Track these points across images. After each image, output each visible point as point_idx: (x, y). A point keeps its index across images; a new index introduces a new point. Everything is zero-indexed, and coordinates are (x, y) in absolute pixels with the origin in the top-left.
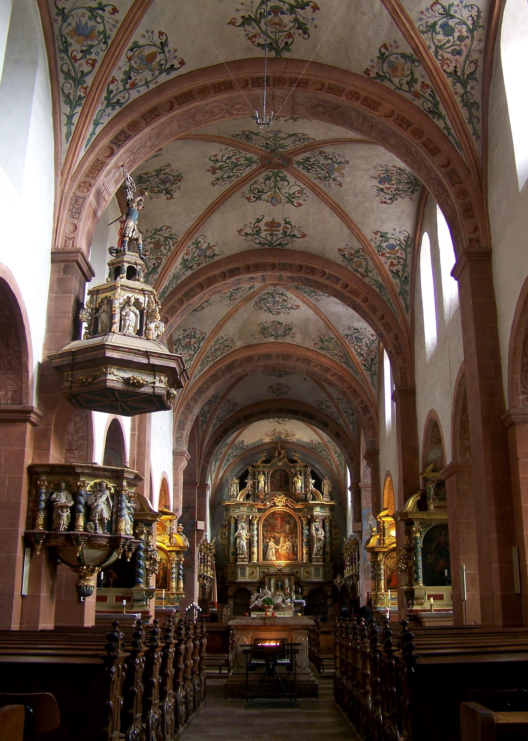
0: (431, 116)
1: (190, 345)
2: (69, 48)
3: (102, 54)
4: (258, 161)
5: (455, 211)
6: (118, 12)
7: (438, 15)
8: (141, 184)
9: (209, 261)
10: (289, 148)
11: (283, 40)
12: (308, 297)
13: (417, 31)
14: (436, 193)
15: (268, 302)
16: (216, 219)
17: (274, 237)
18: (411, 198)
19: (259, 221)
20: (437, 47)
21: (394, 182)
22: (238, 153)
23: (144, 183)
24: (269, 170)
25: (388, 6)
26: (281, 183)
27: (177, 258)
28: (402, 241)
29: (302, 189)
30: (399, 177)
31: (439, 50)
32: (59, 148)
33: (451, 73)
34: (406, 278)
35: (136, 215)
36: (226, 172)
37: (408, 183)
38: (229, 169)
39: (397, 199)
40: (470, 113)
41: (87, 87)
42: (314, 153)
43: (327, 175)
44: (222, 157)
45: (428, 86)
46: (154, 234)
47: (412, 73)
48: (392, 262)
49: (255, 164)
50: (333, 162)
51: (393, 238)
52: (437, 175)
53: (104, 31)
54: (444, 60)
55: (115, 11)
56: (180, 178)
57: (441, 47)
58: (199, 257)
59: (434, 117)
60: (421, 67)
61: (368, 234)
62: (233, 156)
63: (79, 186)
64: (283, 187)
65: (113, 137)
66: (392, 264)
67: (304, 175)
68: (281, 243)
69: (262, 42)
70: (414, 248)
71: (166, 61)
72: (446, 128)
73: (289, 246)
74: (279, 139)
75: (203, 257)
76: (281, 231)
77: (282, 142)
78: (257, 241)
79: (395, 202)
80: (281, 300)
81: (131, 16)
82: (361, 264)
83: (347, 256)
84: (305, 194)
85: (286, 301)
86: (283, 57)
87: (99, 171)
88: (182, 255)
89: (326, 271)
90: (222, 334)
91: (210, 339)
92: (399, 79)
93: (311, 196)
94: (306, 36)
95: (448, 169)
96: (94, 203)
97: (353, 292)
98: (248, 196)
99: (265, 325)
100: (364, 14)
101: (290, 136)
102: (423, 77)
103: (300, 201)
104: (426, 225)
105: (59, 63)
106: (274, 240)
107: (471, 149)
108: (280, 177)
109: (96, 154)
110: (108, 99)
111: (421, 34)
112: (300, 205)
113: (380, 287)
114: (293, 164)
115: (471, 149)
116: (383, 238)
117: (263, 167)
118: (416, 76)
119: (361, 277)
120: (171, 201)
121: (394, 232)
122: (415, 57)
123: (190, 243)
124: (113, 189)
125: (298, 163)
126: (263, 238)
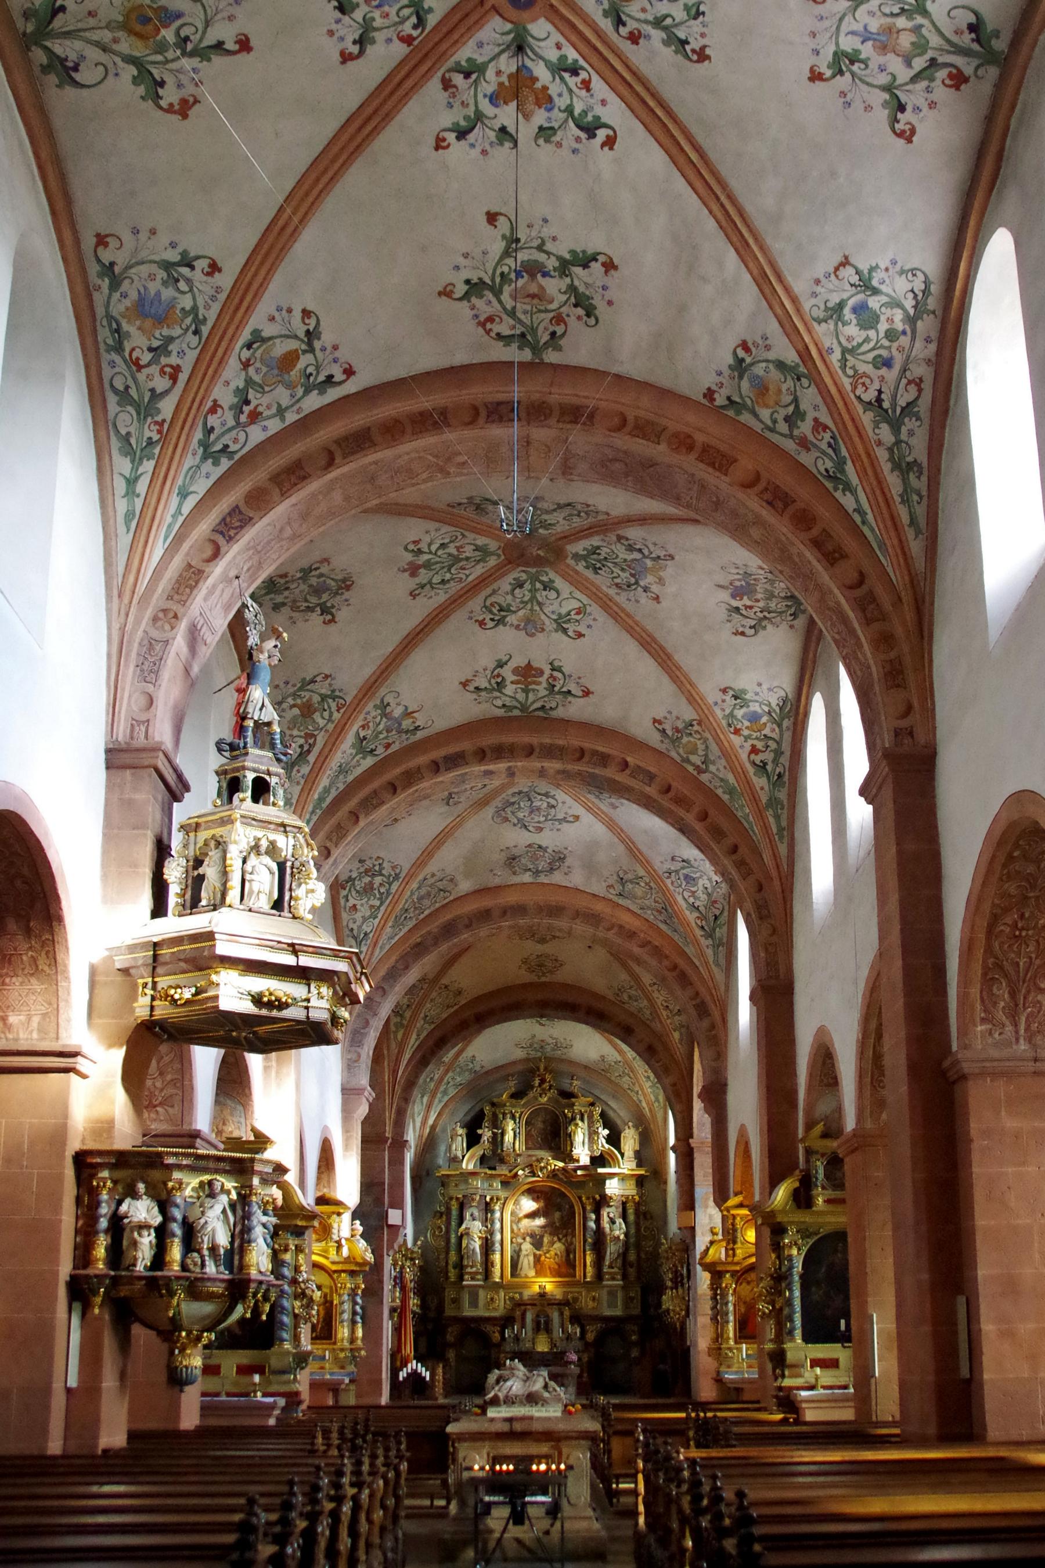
0: (829, 485)
1: (372, 889)
2: (126, 343)
3: (192, 355)
4: (500, 552)
5: (871, 674)
6: (220, 270)
7: (849, 287)
10: (559, 529)
11: (546, 329)
12: (596, 801)
13: (807, 317)
14: (837, 637)
15: (520, 808)
16: (419, 660)
18: (791, 627)
19: (501, 665)
20: (844, 351)
21: (759, 596)
23: (278, 592)
25: (751, 265)
26: (544, 593)
27: (347, 733)
30: (769, 588)
31: (848, 357)
32: (113, 543)
33: (870, 403)
34: (780, 775)
35: (265, 675)
37: (786, 598)
39: (764, 628)
40: (905, 481)
41: (164, 421)
43: (633, 580)
44: (429, 545)
45: (825, 428)
46: (301, 689)
47: (796, 401)
48: (753, 746)
49: (493, 558)
50: (644, 556)
52: (838, 603)
53: (195, 309)
54: (857, 377)
55: (214, 268)
57: (852, 351)
59: (836, 489)
60: (813, 390)
61: (709, 692)
63: (155, 619)
65: (217, 521)
66: (754, 750)
67: (587, 579)
69: (507, 332)
70: (796, 719)
71: (318, 368)
72: (859, 510)
73: (560, 713)
76: (545, 685)
77: (545, 517)
78: (499, 703)
79: (762, 633)
80: (545, 805)
81: (247, 279)
83: (669, 733)
85: (553, 807)
86: (547, 360)
87: (192, 588)
88: (355, 728)
89: (629, 759)
90: (433, 867)
91: (411, 876)
92: (770, 411)
93: (601, 619)
94: (592, 321)
95: (859, 592)
96: (184, 650)
97: (680, 801)
98: (481, 618)
99: (516, 852)
100: (704, 279)
101: (560, 507)
102: (816, 408)
104: (820, 680)
105: (107, 373)
106: (530, 700)
107: (904, 553)
109: (187, 554)
110: (205, 444)
111: (815, 324)
112: (580, 635)
113: (731, 791)
115: (904, 553)
117: (510, 563)
118: (803, 407)
119: (695, 773)
120: (332, 627)
121: (758, 689)
122: (802, 369)
123: (370, 706)
124: (221, 622)
125: (576, 557)
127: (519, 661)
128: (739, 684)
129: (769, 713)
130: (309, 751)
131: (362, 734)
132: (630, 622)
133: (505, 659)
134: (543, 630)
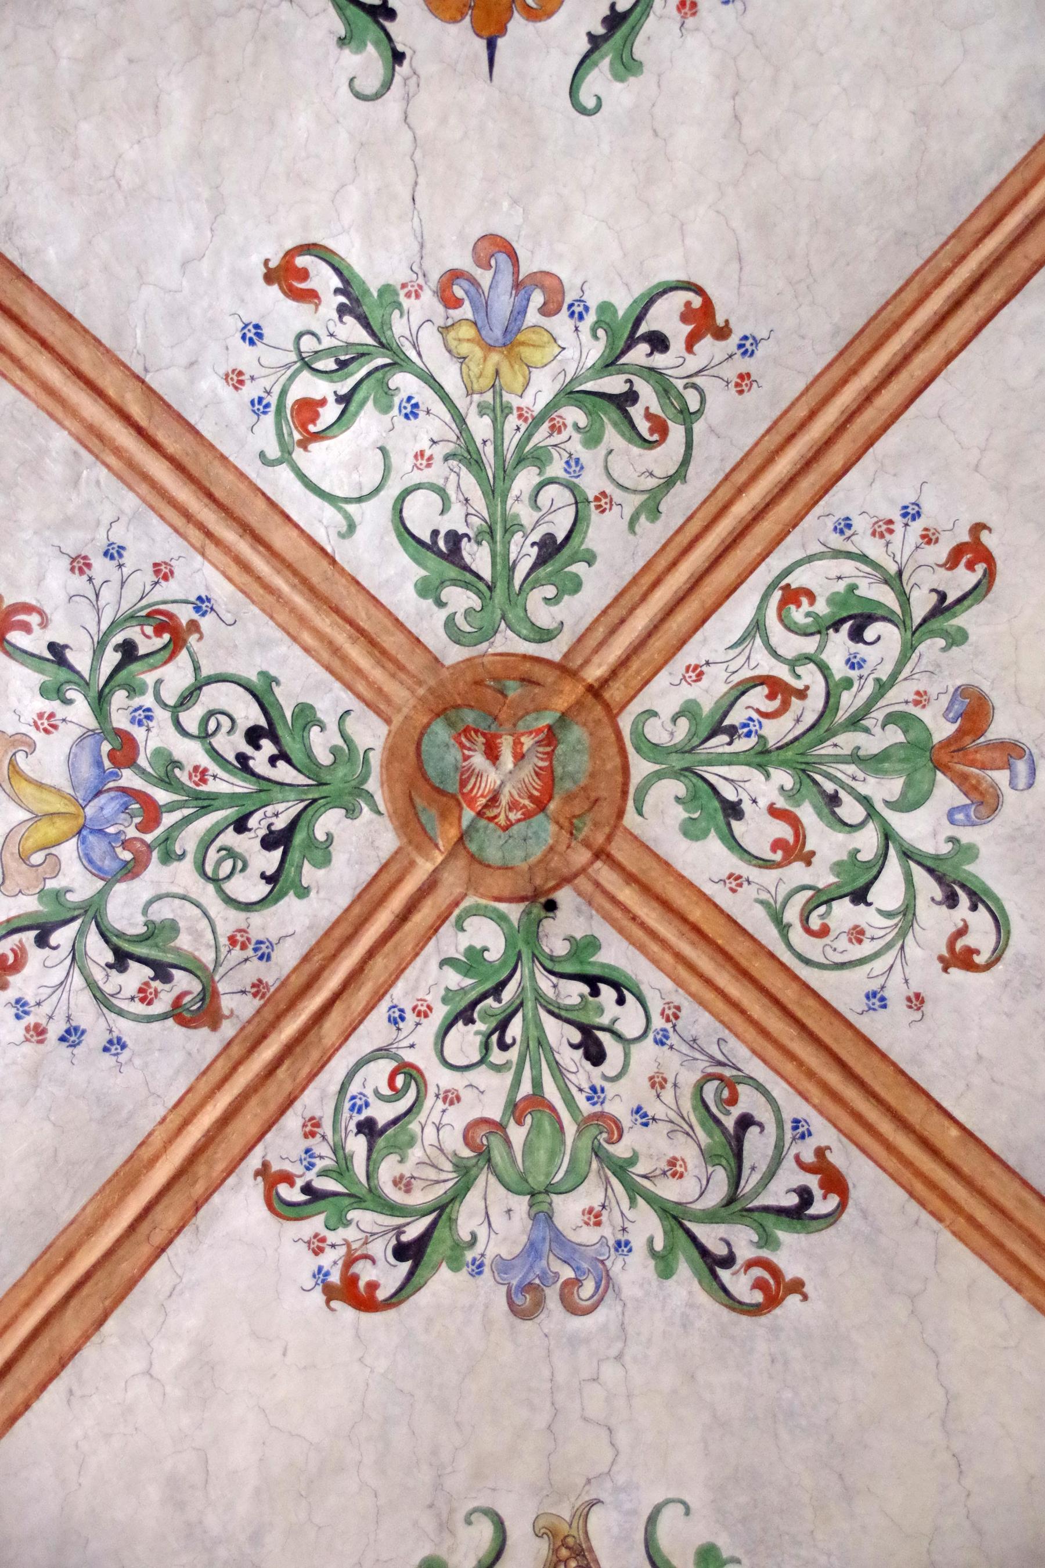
4: (641, 768)
22: (792, 915)
24: (553, 651)
26: (454, 521)
29: (286, 457)
38: (855, 722)
42: (254, 970)
44: (907, 912)
49: (657, 732)
62: (823, 898)
64: (435, 474)
74: (517, 1134)
84: (259, 406)
93: (211, 384)
98: (707, 346)
108: (470, 578)
114: (392, 753)
117: (595, 691)
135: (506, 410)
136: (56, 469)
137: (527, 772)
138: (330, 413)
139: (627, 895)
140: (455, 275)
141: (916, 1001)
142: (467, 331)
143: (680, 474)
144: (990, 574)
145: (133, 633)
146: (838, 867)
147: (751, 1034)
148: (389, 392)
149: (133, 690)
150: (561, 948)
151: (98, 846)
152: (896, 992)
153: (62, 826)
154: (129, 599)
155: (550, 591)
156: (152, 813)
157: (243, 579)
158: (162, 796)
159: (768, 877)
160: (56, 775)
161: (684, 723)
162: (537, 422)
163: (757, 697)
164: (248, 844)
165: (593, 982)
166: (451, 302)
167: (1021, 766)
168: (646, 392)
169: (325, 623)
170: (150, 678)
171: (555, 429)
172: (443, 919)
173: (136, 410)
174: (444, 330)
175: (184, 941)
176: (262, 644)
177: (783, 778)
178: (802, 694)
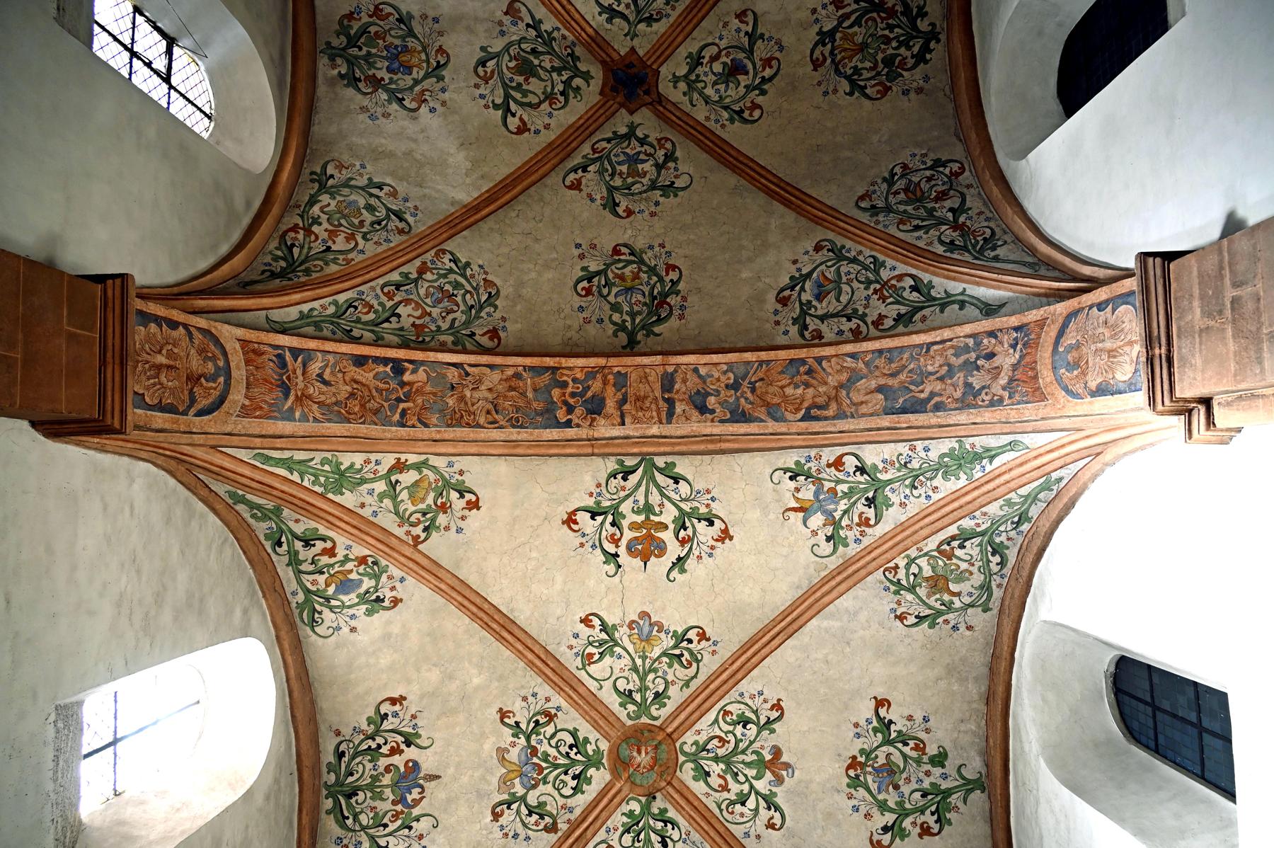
4: (682, 758)
8: (945, 785)
9: (809, 459)
16: (783, 594)
17: (642, 502)
18: (338, 733)
21: (387, 780)
22: (723, 806)
24: (657, 723)
26: (631, 687)
28: (323, 608)
29: (584, 668)
36: (751, 743)
38: (743, 752)
42: (568, 816)
44: (756, 810)
49: (687, 748)
51: (349, 607)
56: (852, 773)
58: (833, 491)
61: (416, 592)
62: (733, 803)
64: (626, 674)
68: (625, 479)
75: (827, 485)
78: (684, 488)
79: (371, 712)
82: (411, 496)
84: (577, 654)
88: (880, 530)
93: (563, 648)
98: (704, 643)
103: (588, 631)
106: (643, 489)
112: (586, 621)
114: (610, 751)
116: (374, 597)
117: (669, 735)
119: (403, 457)
120: (881, 693)
121: (353, 623)
123: (853, 549)
126: (669, 499)
127: (660, 565)
128: (381, 617)
129: (328, 600)
130: (953, 538)
131: (870, 513)
132: (530, 656)
133: (675, 574)
134: (630, 627)
135: (647, 657)
136: (519, 673)
137: (648, 757)
138: (597, 657)
139: (676, 796)
140: (633, 622)
141: (758, 837)
142: (636, 636)
143: (695, 676)
144: (782, 714)
145: (538, 717)
146: (737, 794)
147: (710, 841)
148: (614, 652)
149: (538, 734)
150: (656, 811)
151: (525, 779)
152: (752, 833)
153: (516, 774)
154: (538, 707)
155: (657, 706)
156: (541, 770)
157: (571, 701)
158: (544, 765)
159: (717, 795)
160: (515, 760)
161: (694, 747)
162: (655, 661)
163: (715, 742)
164: (568, 778)
165: (665, 822)
166: (631, 628)
167: (790, 770)
168: (686, 653)
169: (593, 714)
170: (542, 731)
171: (660, 663)
172: (623, 801)
173: (543, 656)
174: (629, 636)
175: (548, 808)
176: (574, 719)
177: (722, 766)
178: (728, 742)
